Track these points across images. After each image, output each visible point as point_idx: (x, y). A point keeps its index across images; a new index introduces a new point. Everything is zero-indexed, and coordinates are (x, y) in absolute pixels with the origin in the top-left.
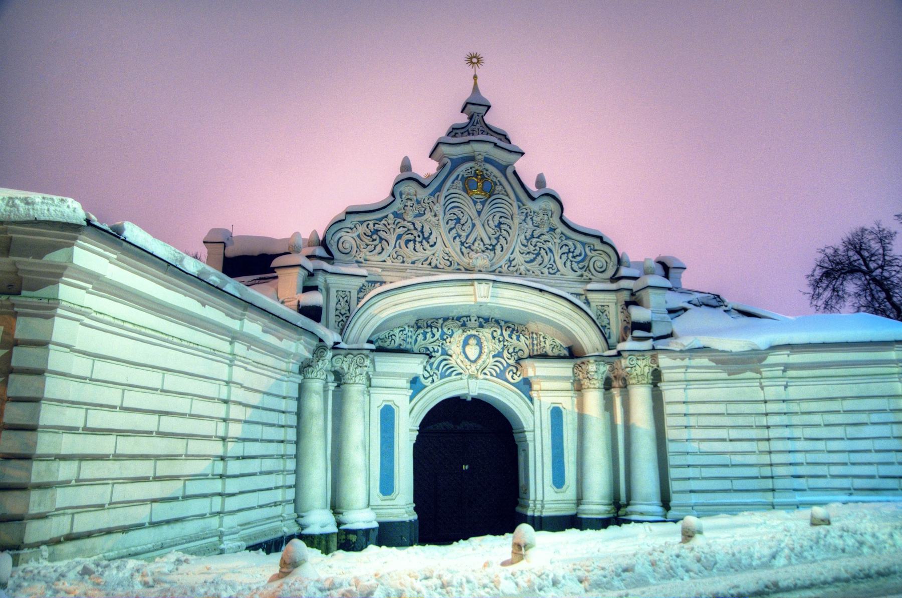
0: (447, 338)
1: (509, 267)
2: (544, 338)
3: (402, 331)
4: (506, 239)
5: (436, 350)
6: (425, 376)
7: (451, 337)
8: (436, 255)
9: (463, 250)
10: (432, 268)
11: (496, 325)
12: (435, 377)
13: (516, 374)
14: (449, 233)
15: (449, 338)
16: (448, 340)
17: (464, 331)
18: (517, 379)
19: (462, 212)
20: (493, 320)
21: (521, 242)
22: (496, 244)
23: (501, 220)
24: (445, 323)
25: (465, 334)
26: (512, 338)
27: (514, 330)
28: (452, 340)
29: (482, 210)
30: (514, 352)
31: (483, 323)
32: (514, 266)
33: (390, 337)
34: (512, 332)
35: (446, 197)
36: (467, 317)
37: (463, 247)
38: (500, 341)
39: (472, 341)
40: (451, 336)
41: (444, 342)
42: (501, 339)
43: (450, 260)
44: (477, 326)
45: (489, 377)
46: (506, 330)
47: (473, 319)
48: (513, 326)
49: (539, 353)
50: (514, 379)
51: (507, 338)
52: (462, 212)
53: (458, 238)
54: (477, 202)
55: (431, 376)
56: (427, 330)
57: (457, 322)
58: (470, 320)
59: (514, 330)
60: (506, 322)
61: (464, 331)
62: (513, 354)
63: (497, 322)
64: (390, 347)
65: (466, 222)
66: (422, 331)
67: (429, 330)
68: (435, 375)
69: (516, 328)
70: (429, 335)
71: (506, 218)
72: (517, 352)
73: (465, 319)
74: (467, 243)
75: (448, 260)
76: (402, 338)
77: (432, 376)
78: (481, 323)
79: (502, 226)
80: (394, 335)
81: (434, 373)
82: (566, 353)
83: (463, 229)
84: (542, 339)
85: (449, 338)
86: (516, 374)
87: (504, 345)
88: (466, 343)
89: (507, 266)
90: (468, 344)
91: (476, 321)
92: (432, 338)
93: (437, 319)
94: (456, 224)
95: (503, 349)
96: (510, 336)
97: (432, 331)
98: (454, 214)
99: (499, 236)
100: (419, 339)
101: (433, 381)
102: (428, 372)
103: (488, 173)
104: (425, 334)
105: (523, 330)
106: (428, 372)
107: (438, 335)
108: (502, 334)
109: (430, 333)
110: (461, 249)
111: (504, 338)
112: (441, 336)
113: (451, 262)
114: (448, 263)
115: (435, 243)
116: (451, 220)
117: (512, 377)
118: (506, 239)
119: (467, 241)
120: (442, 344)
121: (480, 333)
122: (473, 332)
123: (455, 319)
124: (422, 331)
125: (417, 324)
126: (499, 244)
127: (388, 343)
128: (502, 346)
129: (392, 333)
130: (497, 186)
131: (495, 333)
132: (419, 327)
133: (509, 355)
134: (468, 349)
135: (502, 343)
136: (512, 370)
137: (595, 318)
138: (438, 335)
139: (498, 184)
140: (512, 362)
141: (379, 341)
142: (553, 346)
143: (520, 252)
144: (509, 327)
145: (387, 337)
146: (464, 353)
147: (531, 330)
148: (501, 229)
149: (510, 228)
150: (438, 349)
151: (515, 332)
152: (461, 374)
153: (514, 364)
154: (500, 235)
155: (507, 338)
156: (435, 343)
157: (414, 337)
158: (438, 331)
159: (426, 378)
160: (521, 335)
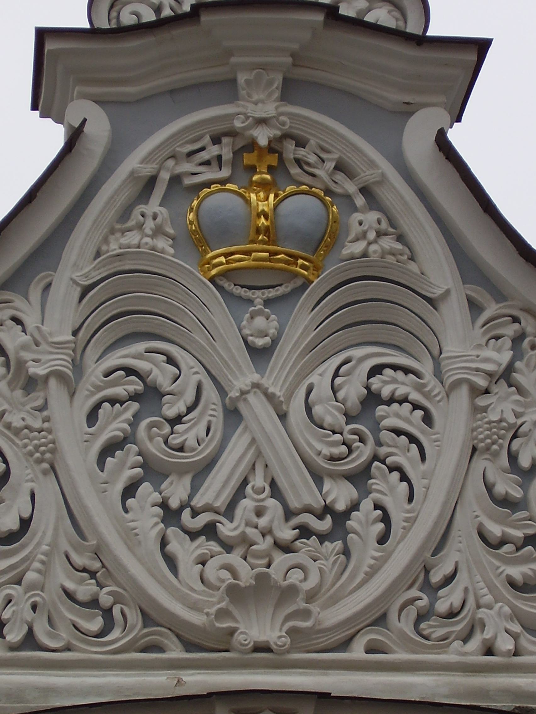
1: (421, 617)
4: (404, 478)
8: (31, 576)
9: (173, 547)
10: (13, 648)
14: (101, 463)
19: (171, 361)
21: (489, 488)
22: (355, 506)
23: (376, 382)
29: (275, 342)
32: (452, 614)
35: (86, 290)
37: (172, 531)
43: (105, 600)
52: (171, 361)
53: (145, 488)
54: (250, 302)
65: (190, 410)
71: (407, 371)
74: (195, 513)
75: (94, 603)
79: (381, 410)
83: (175, 440)
89: (412, 612)
94: (134, 422)
98: (130, 371)
99: (367, 467)
103: (302, 153)
110: (164, 543)
113: (107, 613)
114: (96, 624)
115: (25, 523)
116: (113, 401)
118: (404, 478)
119: (198, 501)
126: (367, 505)
130: (357, 216)
139: (360, 201)
143: (482, 536)
148: (376, 429)
149: (428, 419)
154: (375, 458)
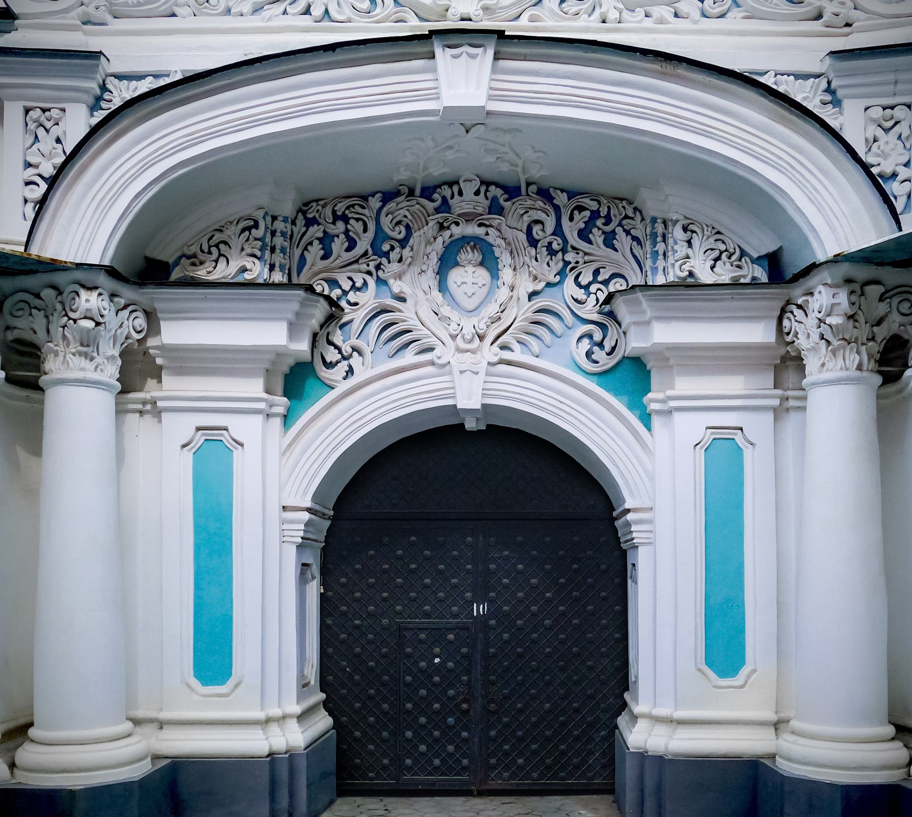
0: (392, 248)
2: (685, 229)
3: (248, 229)
5: (359, 284)
6: (328, 360)
7: (403, 247)
11: (540, 204)
12: (355, 360)
13: (601, 345)
15: (398, 250)
16: (394, 255)
17: (442, 227)
18: (605, 361)
20: (533, 188)
24: (391, 205)
25: (447, 233)
26: (590, 242)
27: (595, 215)
28: (406, 252)
30: (595, 280)
31: (501, 201)
33: (214, 250)
34: (590, 223)
36: (450, 184)
38: (552, 252)
39: (468, 256)
40: (403, 243)
41: (384, 260)
42: (555, 246)
44: (480, 210)
45: (517, 355)
46: (571, 219)
47: (469, 189)
48: (594, 205)
49: (671, 278)
50: (596, 362)
51: (573, 239)
55: (344, 358)
56: (332, 230)
57: (424, 201)
58: (461, 193)
59: (595, 215)
60: (571, 195)
61: (442, 227)
62: (593, 288)
63: (545, 194)
64: (211, 278)
66: (320, 235)
67: (340, 225)
68: (355, 354)
69: (604, 212)
70: (338, 245)
72: (606, 283)
73: (447, 191)
76: (249, 250)
77: (351, 356)
78: (495, 199)
80: (225, 243)
81: (354, 349)
82: (762, 275)
84: (678, 233)
85: (398, 250)
86: (601, 345)
87: (567, 263)
88: (447, 262)
90: (457, 264)
91: (477, 193)
92: (349, 249)
93: (365, 198)
95: (561, 273)
96: (584, 235)
97: (347, 232)
100: (309, 257)
101: (350, 371)
102: (336, 347)
104: (326, 240)
105: (626, 217)
106: (336, 347)
107: (363, 244)
108: (558, 231)
109: (342, 236)
111: (565, 241)
112: (375, 244)
117: (589, 354)
120: (378, 267)
121: (490, 230)
122: (472, 230)
123: (418, 192)
124: (320, 235)
125: (304, 213)
127: (209, 266)
128: (561, 264)
129: (218, 237)
131: (536, 229)
132: (310, 222)
133: (583, 291)
134: (455, 276)
135: (560, 255)
136: (590, 336)
137: (861, 151)
138: (363, 244)
140: (590, 311)
141: (183, 260)
142: (716, 254)
144: (581, 209)
145: (206, 250)
146: (442, 287)
147: (650, 212)
150: (365, 283)
151: (599, 222)
152: (431, 349)
153: (595, 317)
155: (573, 239)
156: (355, 266)
157: (297, 253)
158: (365, 230)
159: (329, 365)
160: (619, 230)
